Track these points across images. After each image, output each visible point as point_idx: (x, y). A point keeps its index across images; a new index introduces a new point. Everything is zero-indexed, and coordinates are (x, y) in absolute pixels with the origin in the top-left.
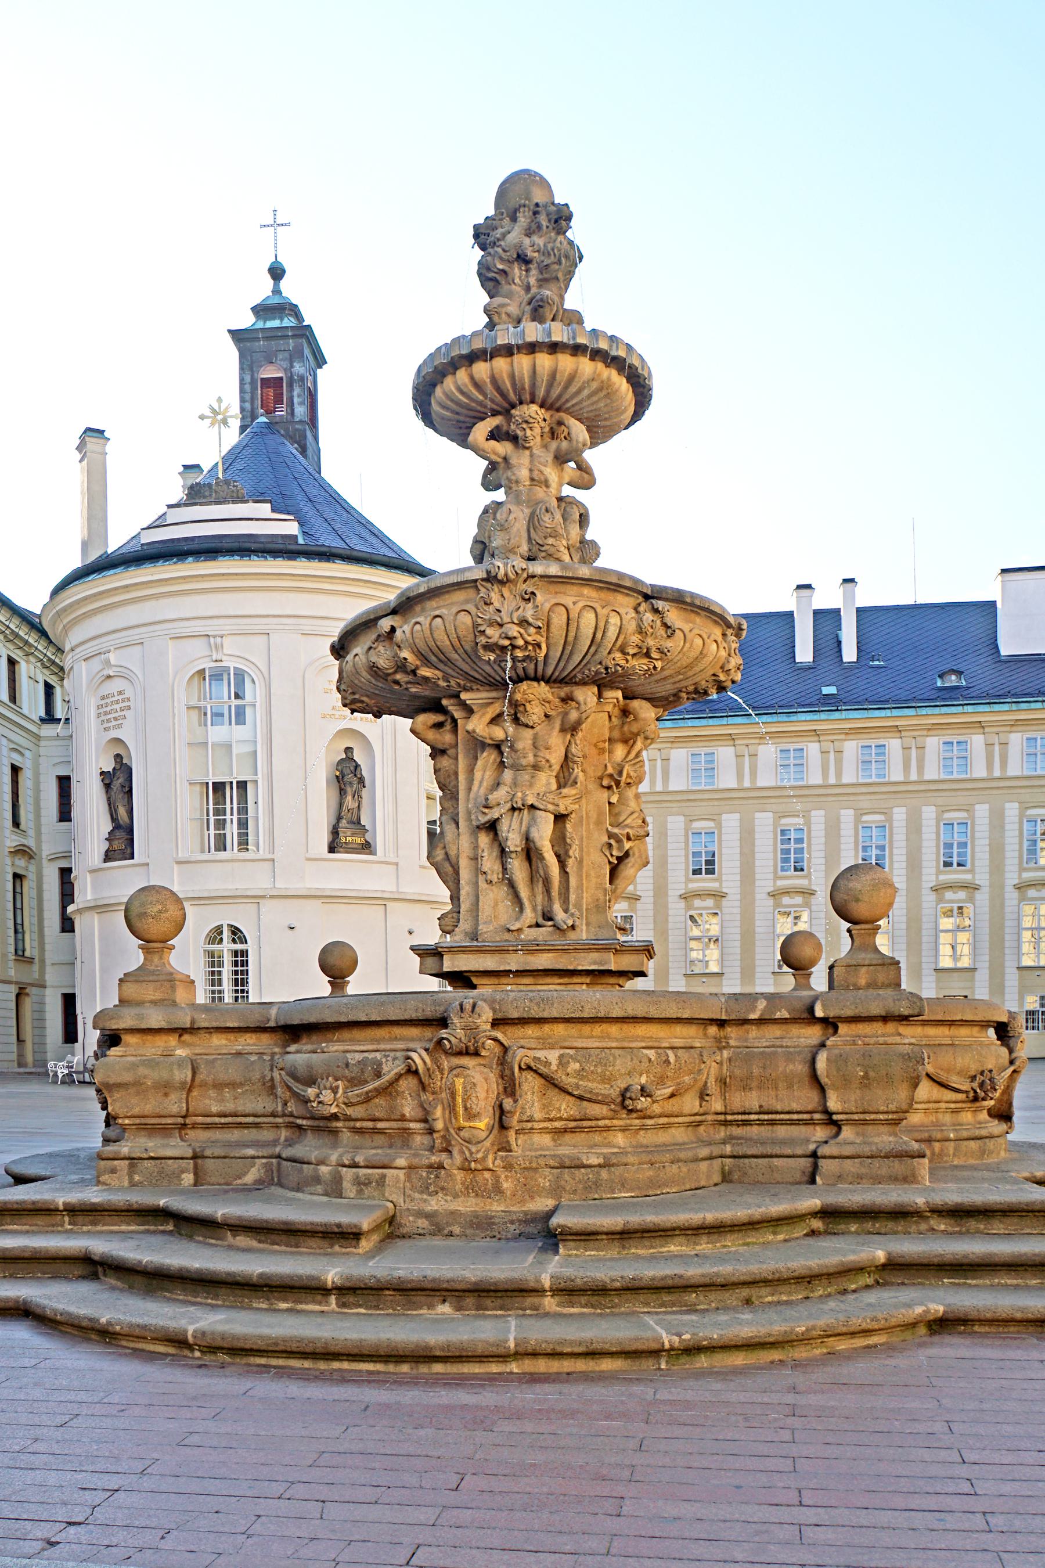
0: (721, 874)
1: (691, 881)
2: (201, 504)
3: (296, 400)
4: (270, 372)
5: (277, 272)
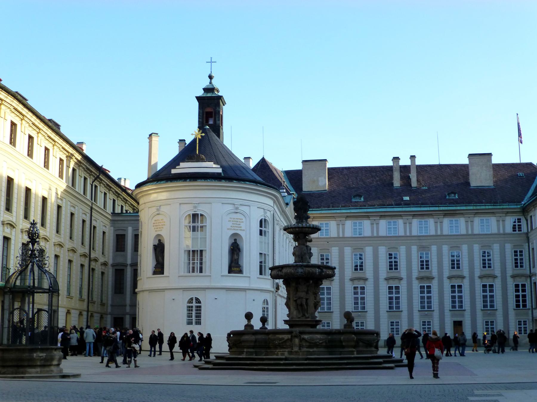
2: (192, 162)
4: (209, 110)
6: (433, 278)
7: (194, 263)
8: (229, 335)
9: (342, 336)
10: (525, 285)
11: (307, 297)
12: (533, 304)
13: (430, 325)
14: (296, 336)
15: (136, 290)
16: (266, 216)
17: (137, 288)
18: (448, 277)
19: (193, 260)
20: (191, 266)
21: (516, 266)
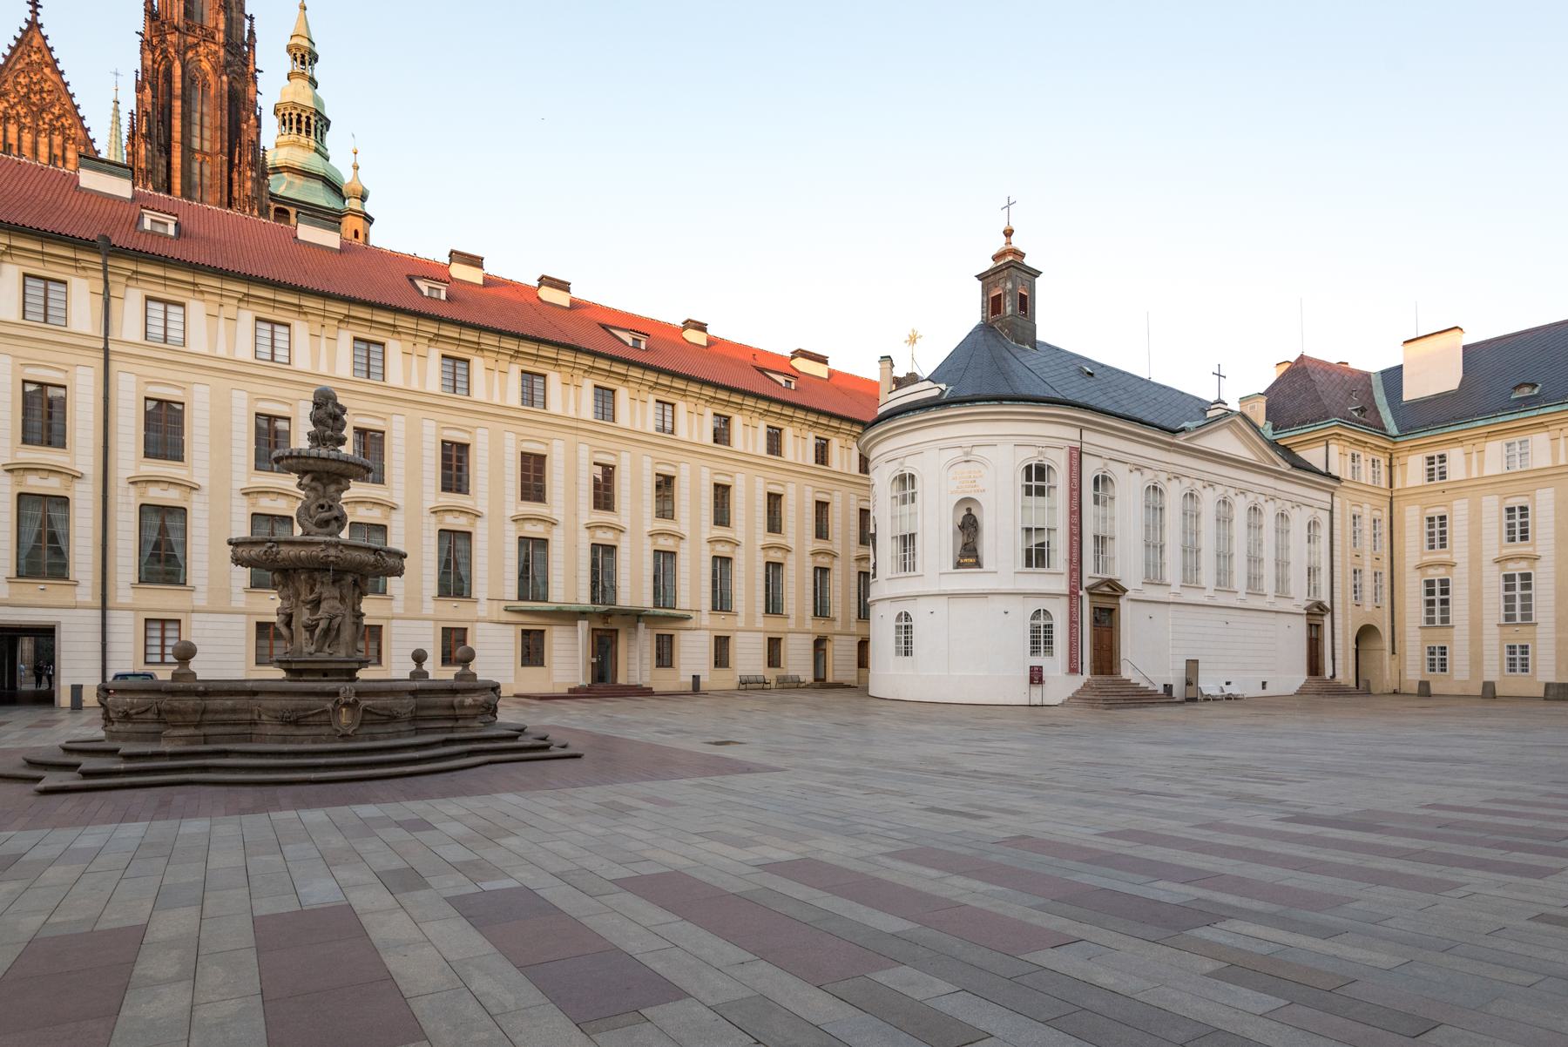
0: (1534, 540)
1: (1506, 547)
3: (1007, 304)
5: (1008, 233)
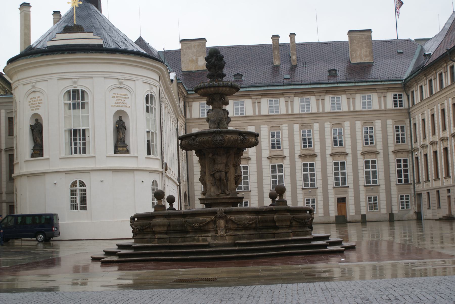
6: (316, 156)
7: (75, 144)
8: (133, 219)
9: (275, 215)
10: (407, 160)
11: (226, 170)
12: (415, 178)
13: (314, 202)
14: (221, 218)
15: (13, 175)
16: (152, 92)
17: (13, 173)
18: (331, 155)
19: (75, 140)
20: (73, 147)
21: (398, 142)
